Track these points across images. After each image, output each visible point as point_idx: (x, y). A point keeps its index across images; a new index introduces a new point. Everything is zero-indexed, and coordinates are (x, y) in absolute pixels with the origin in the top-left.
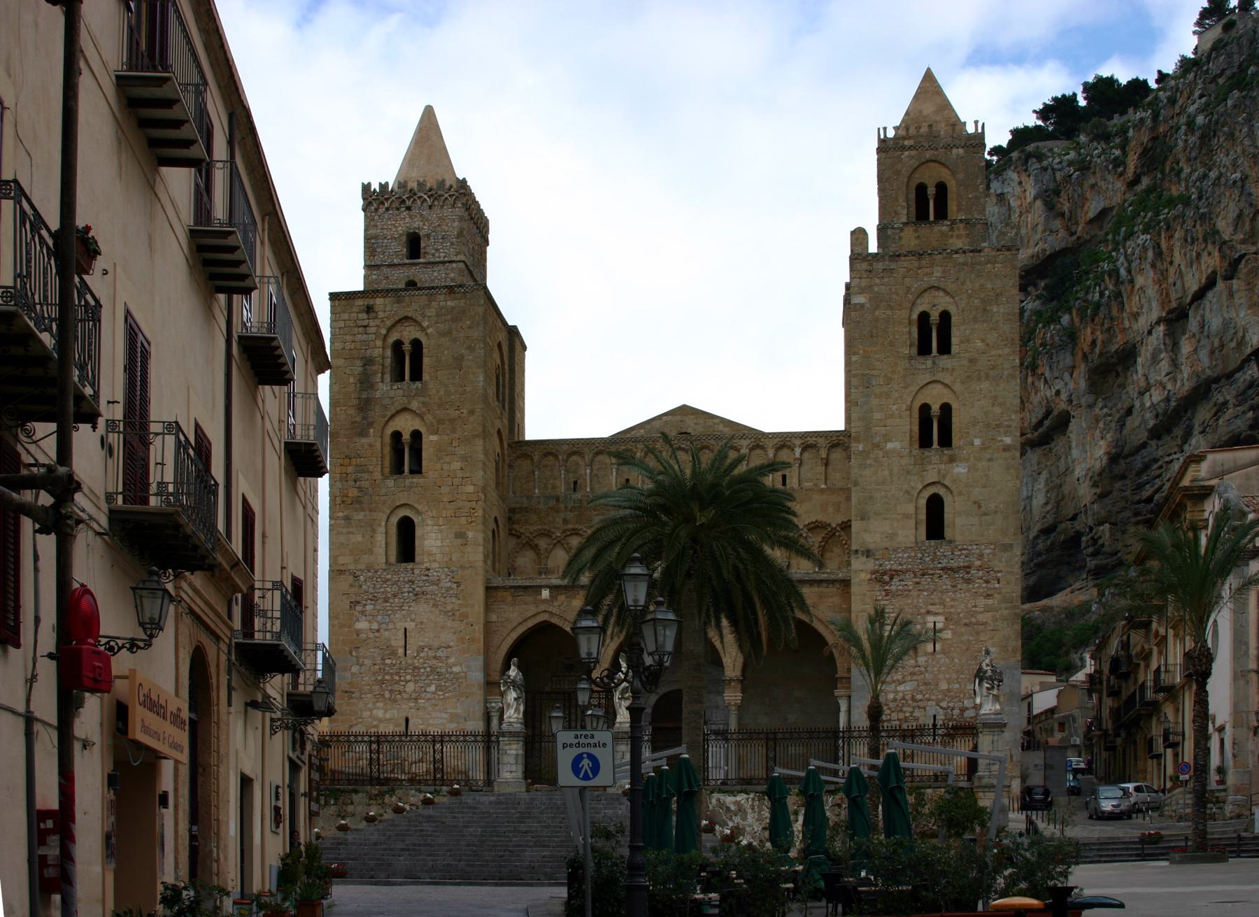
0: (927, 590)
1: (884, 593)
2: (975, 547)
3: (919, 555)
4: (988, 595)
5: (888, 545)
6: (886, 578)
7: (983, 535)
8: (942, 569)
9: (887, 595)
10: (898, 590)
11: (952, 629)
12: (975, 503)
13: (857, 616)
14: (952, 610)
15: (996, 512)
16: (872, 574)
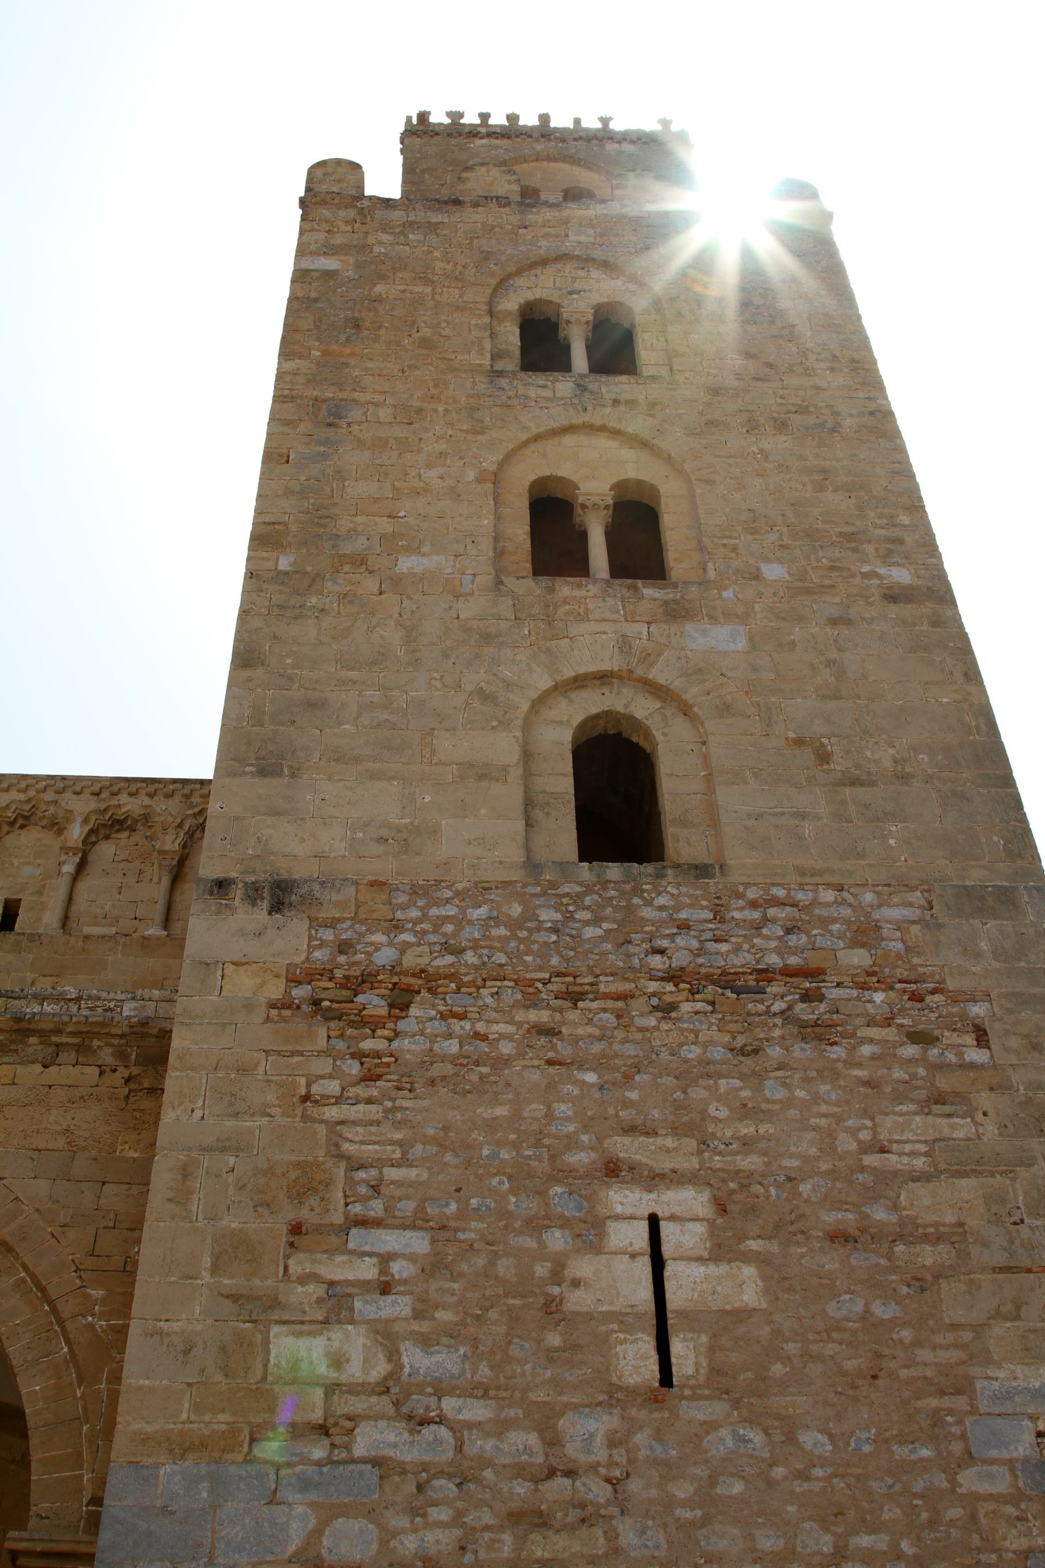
0: (599, 1064)
1: (353, 1068)
2: (828, 896)
3: (548, 915)
4: (940, 1099)
5: (386, 868)
6: (374, 1003)
7: (861, 856)
8: (673, 977)
9: (369, 1078)
10: (431, 1057)
11: (760, 1260)
12: (799, 742)
13: (185, 1172)
14: (750, 1162)
15: (904, 778)
16: (294, 980)
